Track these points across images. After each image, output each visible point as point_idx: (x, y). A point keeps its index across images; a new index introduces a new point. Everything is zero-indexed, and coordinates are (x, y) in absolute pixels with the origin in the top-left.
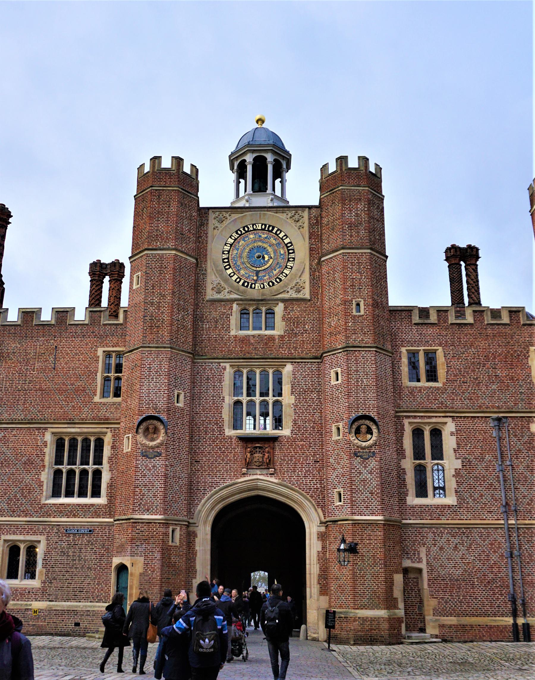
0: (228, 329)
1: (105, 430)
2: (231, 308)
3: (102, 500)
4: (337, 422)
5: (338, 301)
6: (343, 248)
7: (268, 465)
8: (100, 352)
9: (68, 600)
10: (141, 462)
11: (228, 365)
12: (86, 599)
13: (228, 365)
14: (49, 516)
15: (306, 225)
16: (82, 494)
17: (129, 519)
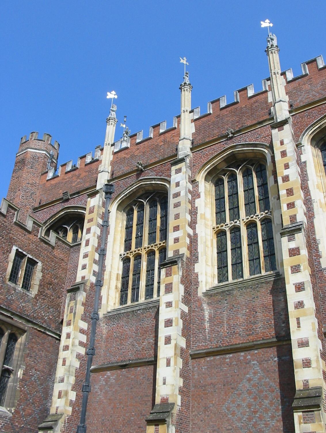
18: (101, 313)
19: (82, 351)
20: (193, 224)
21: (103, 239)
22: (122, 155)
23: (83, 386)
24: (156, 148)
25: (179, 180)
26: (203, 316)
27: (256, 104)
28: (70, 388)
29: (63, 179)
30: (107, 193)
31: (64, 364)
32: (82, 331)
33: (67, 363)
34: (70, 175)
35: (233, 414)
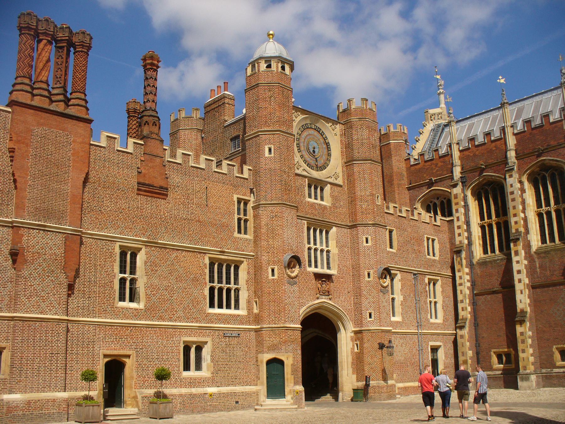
0: (304, 197)
1: (242, 259)
2: (305, 181)
3: (242, 312)
4: (369, 269)
5: (368, 193)
6: (371, 160)
7: (327, 293)
8: (235, 197)
9: (229, 385)
10: (287, 287)
11: (306, 222)
12: (239, 384)
13: (306, 222)
14: (212, 322)
15: (338, 134)
16: (228, 307)
17: (269, 328)
18: (475, 261)
19: (469, 284)
20: (524, 211)
21: (467, 215)
22: (466, 153)
23: (474, 304)
24: (491, 151)
25: (513, 182)
26: (536, 265)
27: (556, 129)
28: (467, 305)
29: (424, 166)
30: (462, 183)
31: (461, 293)
32: (467, 274)
33: (463, 293)
34: (429, 163)
35: (556, 314)
